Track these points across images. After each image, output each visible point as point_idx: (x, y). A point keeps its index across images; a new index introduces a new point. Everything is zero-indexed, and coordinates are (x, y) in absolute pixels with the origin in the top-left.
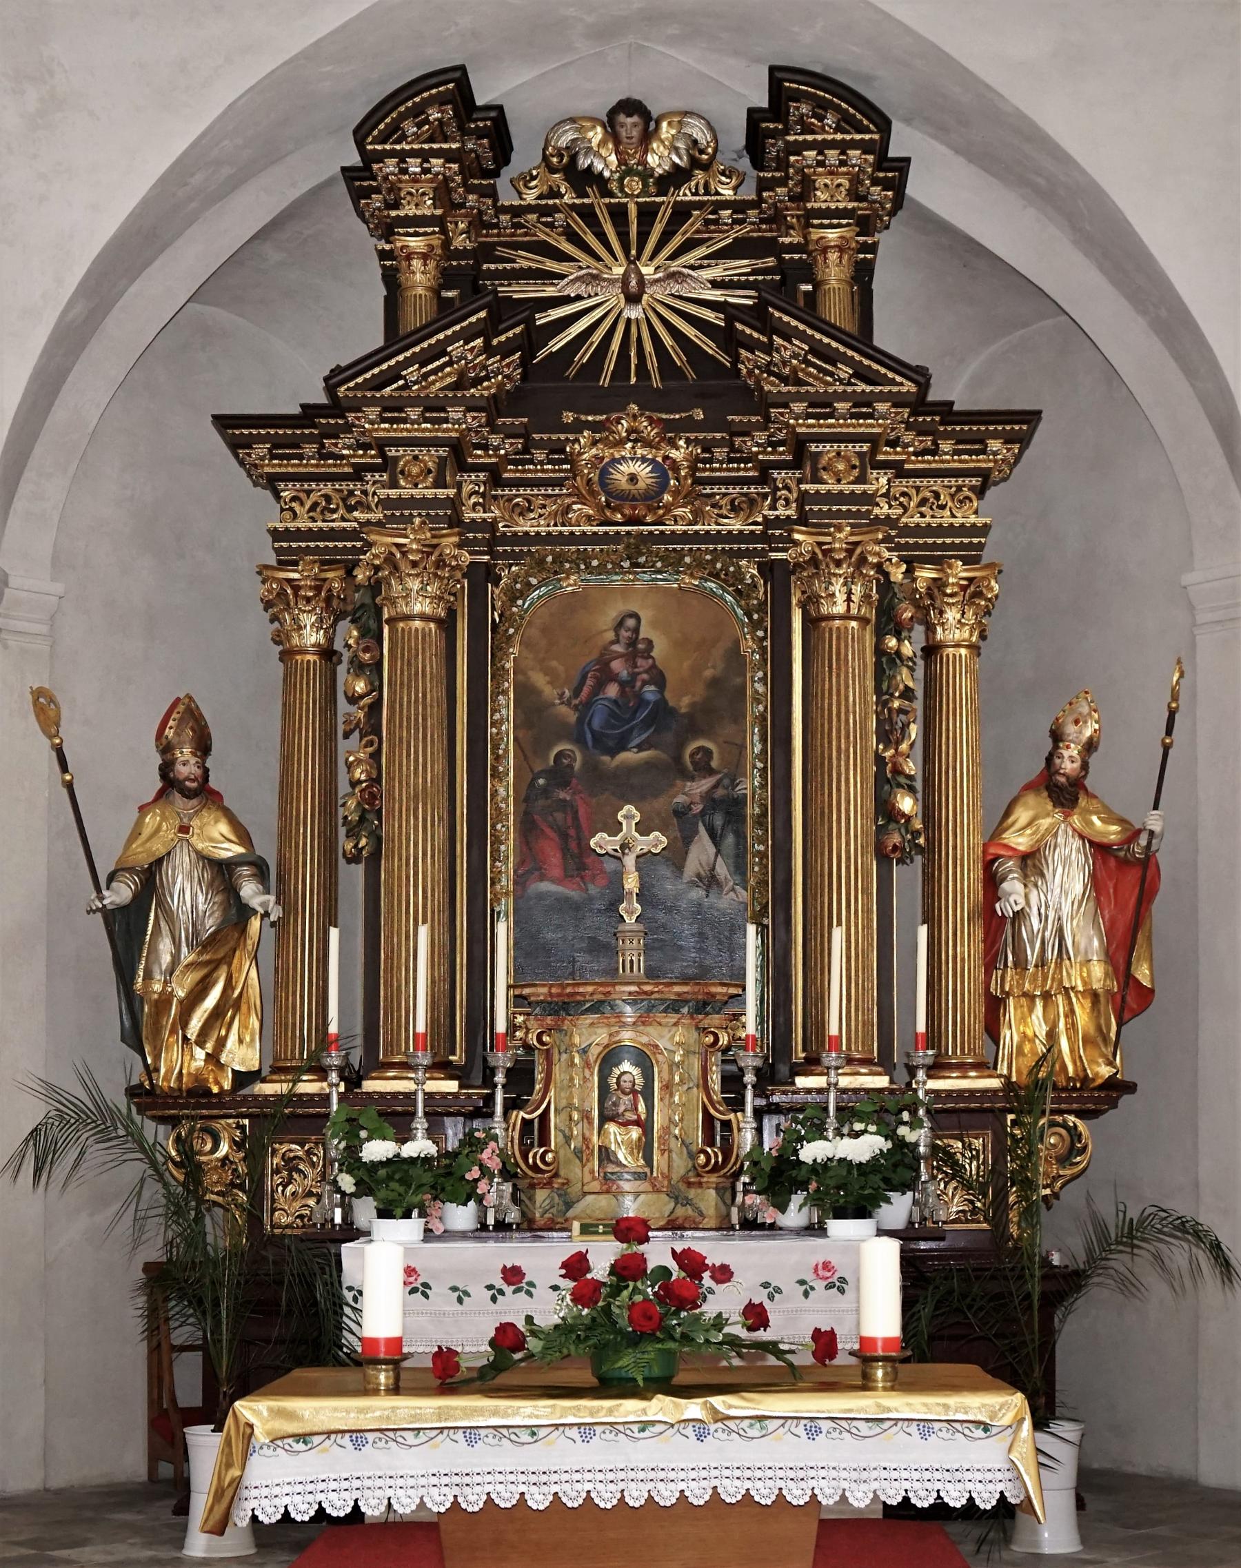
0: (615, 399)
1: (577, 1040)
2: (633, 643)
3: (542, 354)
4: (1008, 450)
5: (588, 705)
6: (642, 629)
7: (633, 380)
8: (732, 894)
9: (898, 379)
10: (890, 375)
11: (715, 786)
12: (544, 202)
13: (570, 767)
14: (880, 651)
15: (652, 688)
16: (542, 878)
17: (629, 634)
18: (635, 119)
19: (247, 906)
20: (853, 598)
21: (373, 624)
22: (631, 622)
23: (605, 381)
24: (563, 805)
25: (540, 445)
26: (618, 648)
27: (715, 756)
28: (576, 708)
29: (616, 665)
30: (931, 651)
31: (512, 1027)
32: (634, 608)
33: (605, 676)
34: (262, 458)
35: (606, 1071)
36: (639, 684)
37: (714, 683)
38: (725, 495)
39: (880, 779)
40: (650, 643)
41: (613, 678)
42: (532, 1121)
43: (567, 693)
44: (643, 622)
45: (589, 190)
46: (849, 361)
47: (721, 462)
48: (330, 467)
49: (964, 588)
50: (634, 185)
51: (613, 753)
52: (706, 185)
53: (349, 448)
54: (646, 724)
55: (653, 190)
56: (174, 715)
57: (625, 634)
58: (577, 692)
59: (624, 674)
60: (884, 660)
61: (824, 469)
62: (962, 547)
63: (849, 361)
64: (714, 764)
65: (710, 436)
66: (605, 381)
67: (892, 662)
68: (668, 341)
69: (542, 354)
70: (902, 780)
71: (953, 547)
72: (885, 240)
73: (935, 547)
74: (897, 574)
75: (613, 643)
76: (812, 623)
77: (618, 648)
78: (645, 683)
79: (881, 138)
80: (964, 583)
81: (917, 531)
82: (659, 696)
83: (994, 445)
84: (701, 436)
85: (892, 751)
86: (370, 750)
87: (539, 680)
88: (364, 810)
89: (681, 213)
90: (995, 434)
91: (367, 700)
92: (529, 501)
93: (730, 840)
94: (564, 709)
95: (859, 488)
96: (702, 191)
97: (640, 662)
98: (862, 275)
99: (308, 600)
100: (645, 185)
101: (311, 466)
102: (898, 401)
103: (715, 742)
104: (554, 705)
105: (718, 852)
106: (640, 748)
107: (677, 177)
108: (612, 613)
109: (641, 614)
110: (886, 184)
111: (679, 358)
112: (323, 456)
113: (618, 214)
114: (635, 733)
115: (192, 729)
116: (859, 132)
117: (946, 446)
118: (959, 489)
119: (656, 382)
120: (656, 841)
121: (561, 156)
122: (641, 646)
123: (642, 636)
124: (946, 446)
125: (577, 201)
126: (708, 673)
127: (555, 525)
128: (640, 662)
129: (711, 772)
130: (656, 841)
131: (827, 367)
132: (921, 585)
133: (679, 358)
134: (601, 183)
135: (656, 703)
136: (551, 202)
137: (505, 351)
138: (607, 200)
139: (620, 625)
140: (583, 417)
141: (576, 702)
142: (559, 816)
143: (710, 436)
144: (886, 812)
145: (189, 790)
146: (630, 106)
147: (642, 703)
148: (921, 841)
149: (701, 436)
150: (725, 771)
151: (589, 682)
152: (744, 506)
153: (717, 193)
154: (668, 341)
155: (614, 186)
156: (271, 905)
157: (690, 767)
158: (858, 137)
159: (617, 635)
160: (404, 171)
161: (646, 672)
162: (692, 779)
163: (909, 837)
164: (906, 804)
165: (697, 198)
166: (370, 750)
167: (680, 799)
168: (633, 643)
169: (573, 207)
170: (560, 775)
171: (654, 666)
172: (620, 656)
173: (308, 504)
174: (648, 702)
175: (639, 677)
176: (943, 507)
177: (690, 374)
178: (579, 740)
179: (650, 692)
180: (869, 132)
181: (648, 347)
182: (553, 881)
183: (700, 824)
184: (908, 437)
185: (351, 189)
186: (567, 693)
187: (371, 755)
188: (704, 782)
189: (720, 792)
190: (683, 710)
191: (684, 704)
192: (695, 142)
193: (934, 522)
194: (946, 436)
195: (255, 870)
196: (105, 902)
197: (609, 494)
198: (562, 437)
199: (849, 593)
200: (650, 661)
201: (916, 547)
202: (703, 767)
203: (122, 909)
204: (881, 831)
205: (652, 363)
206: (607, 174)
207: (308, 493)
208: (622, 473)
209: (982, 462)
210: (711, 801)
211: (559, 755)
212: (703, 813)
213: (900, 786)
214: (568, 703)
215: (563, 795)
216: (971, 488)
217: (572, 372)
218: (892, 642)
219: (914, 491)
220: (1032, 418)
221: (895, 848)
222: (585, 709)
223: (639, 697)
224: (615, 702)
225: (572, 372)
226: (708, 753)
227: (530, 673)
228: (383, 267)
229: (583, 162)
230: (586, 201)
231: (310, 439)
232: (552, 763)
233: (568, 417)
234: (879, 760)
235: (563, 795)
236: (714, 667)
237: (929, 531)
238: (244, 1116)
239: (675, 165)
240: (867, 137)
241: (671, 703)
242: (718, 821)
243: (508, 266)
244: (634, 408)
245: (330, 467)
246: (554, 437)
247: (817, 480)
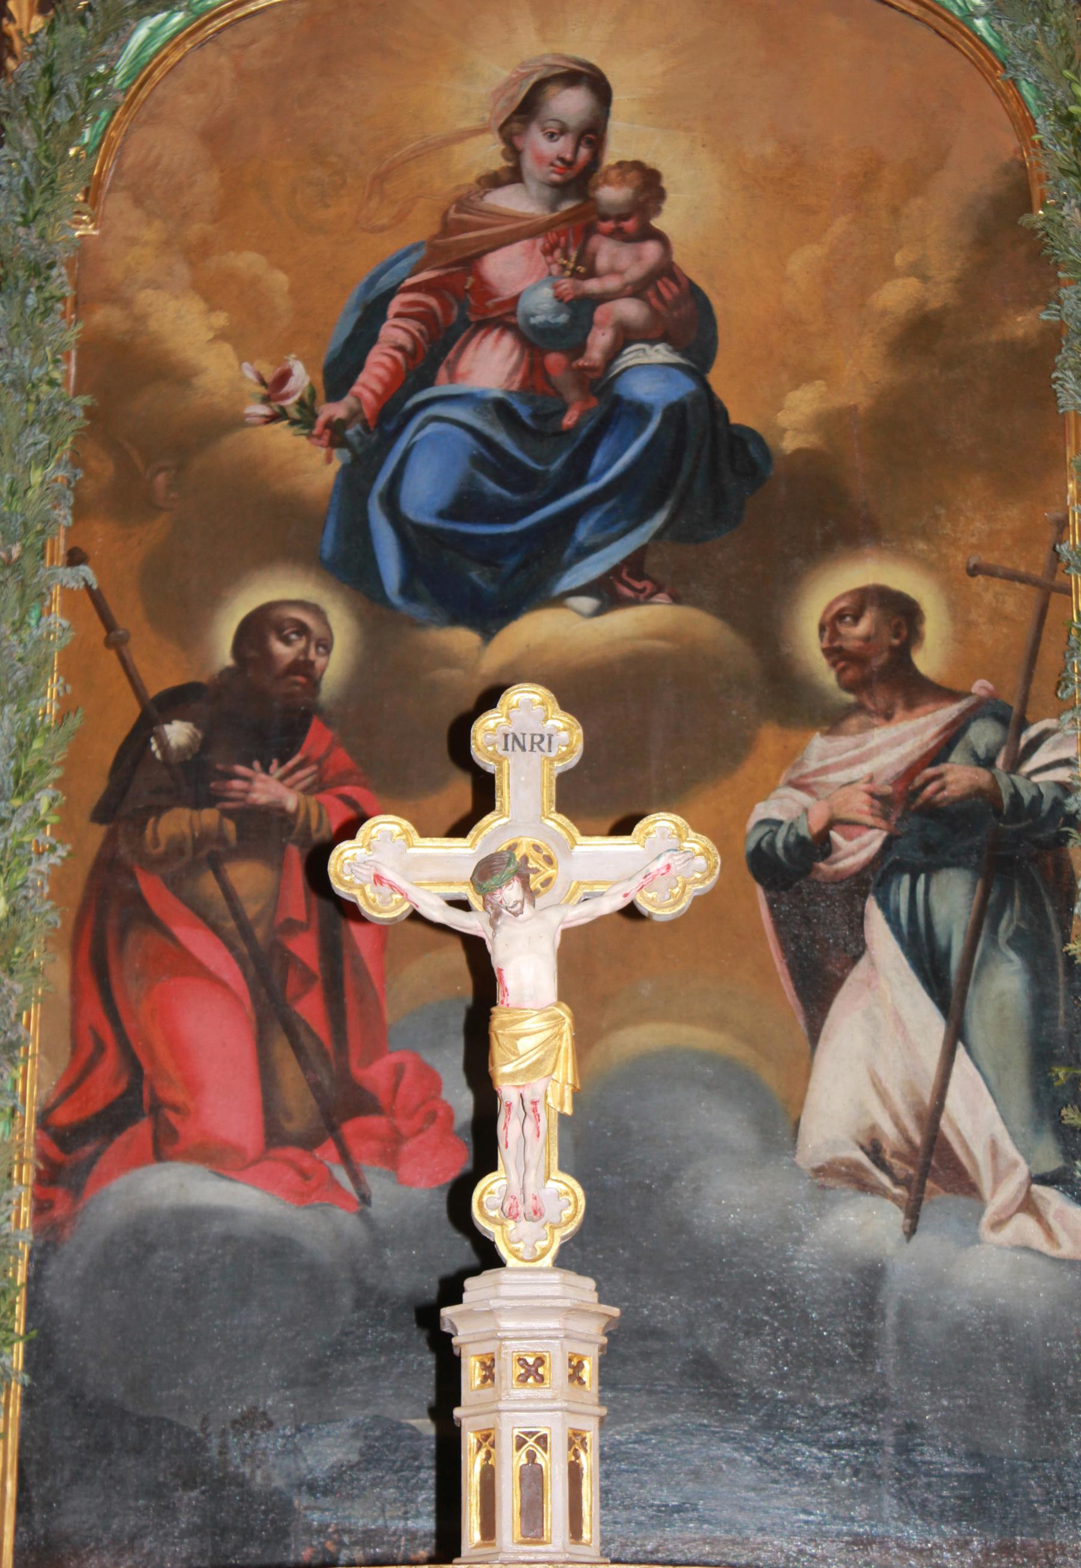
6: (617, 126)
8: (1025, 1226)
11: (939, 754)
13: (304, 668)
15: (661, 354)
17: (562, 146)
36: (600, 340)
43: (301, 378)
75: (494, 181)
78: (626, 336)
82: (683, 387)
103: (929, 566)
104: (238, 422)
109: (614, 72)
114: (583, 532)
123: (615, 152)
135: (676, 413)
141: (338, 410)
150: (980, 687)
157: (826, 675)
159: (514, 152)
161: (637, 290)
171: (666, 270)
174: (640, 412)
175: (600, 313)
186: (301, 378)
188: (880, 735)
190: (789, 444)
200: (651, 250)
224: (502, 409)
227: (146, 298)
232: (224, 655)
236: (917, 270)
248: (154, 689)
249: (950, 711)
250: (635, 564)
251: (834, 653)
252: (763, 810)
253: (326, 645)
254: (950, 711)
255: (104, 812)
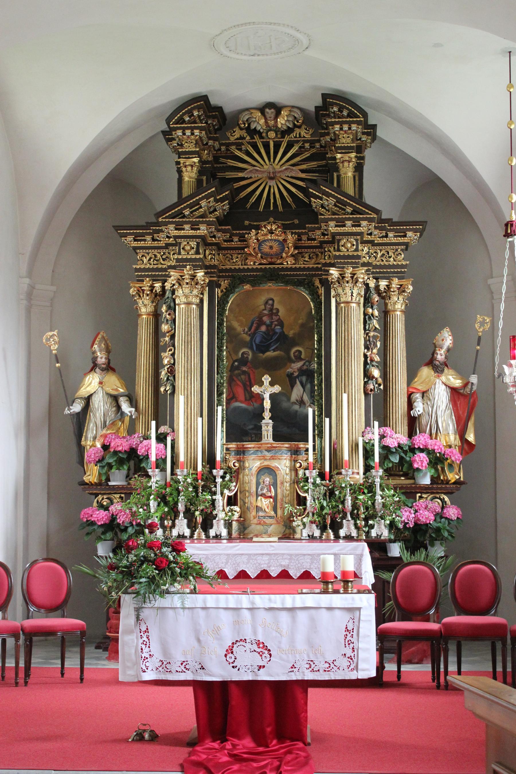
0: (265, 216)
1: (247, 465)
2: (271, 310)
3: (238, 198)
4: (415, 235)
5: (254, 333)
6: (275, 304)
7: (272, 208)
9: (370, 212)
10: (367, 211)
11: (303, 365)
12: (238, 141)
13: (247, 357)
14: (365, 314)
15: (279, 327)
16: (236, 401)
17: (269, 306)
18: (273, 110)
19: (124, 412)
20: (354, 295)
21: (172, 304)
22: (270, 302)
23: (261, 208)
24: (244, 372)
25: (236, 235)
26: (265, 312)
27: (303, 354)
28: (249, 335)
29: (265, 319)
30: (386, 313)
31: (225, 460)
32: (272, 296)
33: (261, 323)
34: (131, 241)
35: (259, 477)
36: (273, 326)
37: (302, 325)
38: (307, 252)
39: (366, 363)
40: (278, 310)
41: (264, 323)
42: (231, 496)
43: (246, 330)
44: (275, 302)
45: (255, 137)
46: (351, 205)
47: (305, 241)
48: (155, 244)
49: (399, 289)
50: (272, 135)
51: (264, 352)
52: (300, 134)
53: (163, 238)
54: (277, 340)
55: (279, 136)
56: (98, 339)
57: (268, 307)
58: (250, 329)
59: (268, 322)
60: (367, 317)
61: (342, 246)
62: (397, 273)
63: (351, 205)
64: (302, 357)
65: (300, 231)
66: (261, 208)
67: (370, 318)
68: (285, 193)
69: (238, 198)
70: (374, 363)
71: (394, 273)
72: (367, 153)
73: (387, 273)
74: (372, 284)
75: (264, 310)
76: (338, 304)
77: (265, 312)
78: (276, 325)
79: (364, 120)
80: (399, 286)
81: (380, 267)
82: (281, 330)
83: (409, 234)
84: (297, 231)
85: (370, 352)
86: (171, 352)
87: (236, 324)
88: (169, 376)
89: (290, 146)
90: (410, 230)
91: (170, 334)
92: (232, 256)
93: (308, 386)
94: (245, 335)
95: (355, 254)
96: (298, 136)
97: (274, 317)
98: (359, 169)
99: (148, 295)
100: (276, 135)
101: (149, 243)
102: (370, 220)
103: (303, 348)
104: (241, 334)
105: (304, 391)
106: (274, 350)
107: (289, 131)
108: (263, 299)
109: (275, 299)
110: (368, 134)
111: (289, 199)
112: (154, 240)
113: (266, 146)
114: (272, 344)
115: (104, 345)
116: (356, 118)
117: (391, 234)
118: (397, 250)
119: (280, 208)
120: (277, 389)
121: (244, 124)
122: (274, 311)
123: (275, 307)
124: (391, 234)
125: (251, 141)
126: (300, 321)
127: (242, 265)
128: (274, 317)
129: (301, 359)
130: (277, 389)
131: (343, 207)
132: (382, 288)
133: (289, 199)
134: (260, 133)
135: (280, 333)
136: (240, 141)
137: (222, 200)
138: (262, 140)
139: (266, 303)
140: (252, 223)
141: (250, 333)
142: (243, 377)
143: (300, 231)
144: (368, 376)
145: (103, 368)
146: (270, 105)
147: (275, 333)
148: (382, 387)
149: (297, 231)
151: (255, 325)
152: (314, 257)
153: (304, 137)
154: (285, 193)
155: (264, 135)
156: (133, 412)
158: (355, 119)
159: (265, 307)
160: (184, 134)
161: (277, 321)
162: (294, 362)
163: (377, 385)
164: (376, 373)
165: (296, 139)
166: (171, 352)
167: (290, 370)
168: (271, 310)
169: (249, 143)
170: (243, 361)
171: (279, 319)
172: (266, 315)
173: (148, 258)
174: (277, 333)
176: (390, 257)
177: (294, 206)
178: (251, 348)
179: (278, 329)
180: (359, 117)
181: (278, 196)
182: (242, 402)
183: (297, 380)
184: (376, 232)
185: (165, 139)
187: (171, 355)
188: (298, 363)
189: (305, 367)
190: (290, 336)
191: (291, 333)
192: (295, 118)
193: (387, 263)
194: (391, 230)
195: (127, 398)
196: (71, 411)
197: (262, 253)
198: (244, 232)
199: (352, 293)
200: (278, 317)
201: (380, 273)
202: (298, 358)
203: (78, 414)
204: (366, 383)
205: (279, 202)
206: (261, 131)
207: (148, 254)
208: (267, 245)
209: (405, 240)
210: (302, 372)
211: (243, 353)
212: (297, 377)
213: (373, 366)
214: (247, 333)
215: (244, 369)
216: (402, 250)
217: (248, 206)
218: (370, 310)
219: (379, 251)
220: (423, 223)
221: (371, 390)
222: (253, 336)
223: (273, 330)
224: (264, 332)
225: (248, 206)
226: (300, 352)
227: (232, 322)
228: (177, 167)
229: (253, 127)
230: (254, 140)
231: (149, 234)
232: (240, 356)
233: (247, 223)
234: (365, 356)
235: (244, 369)
236: (302, 319)
237: (385, 266)
238: (123, 493)
239: (288, 127)
240: (358, 119)
241: (286, 333)
242: (304, 379)
243: (225, 165)
244: (272, 219)
245: (155, 244)
246: (241, 232)
247: (339, 250)
248: (235, 358)
249: (304, 361)
250: (276, 348)
251: (294, 356)
252: (288, 371)
253: (249, 355)
254: (304, 361)
255: (230, 371)
